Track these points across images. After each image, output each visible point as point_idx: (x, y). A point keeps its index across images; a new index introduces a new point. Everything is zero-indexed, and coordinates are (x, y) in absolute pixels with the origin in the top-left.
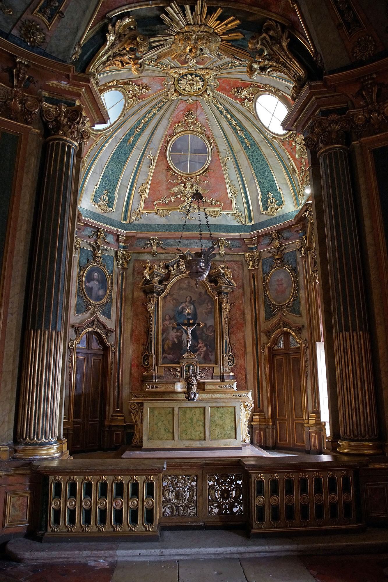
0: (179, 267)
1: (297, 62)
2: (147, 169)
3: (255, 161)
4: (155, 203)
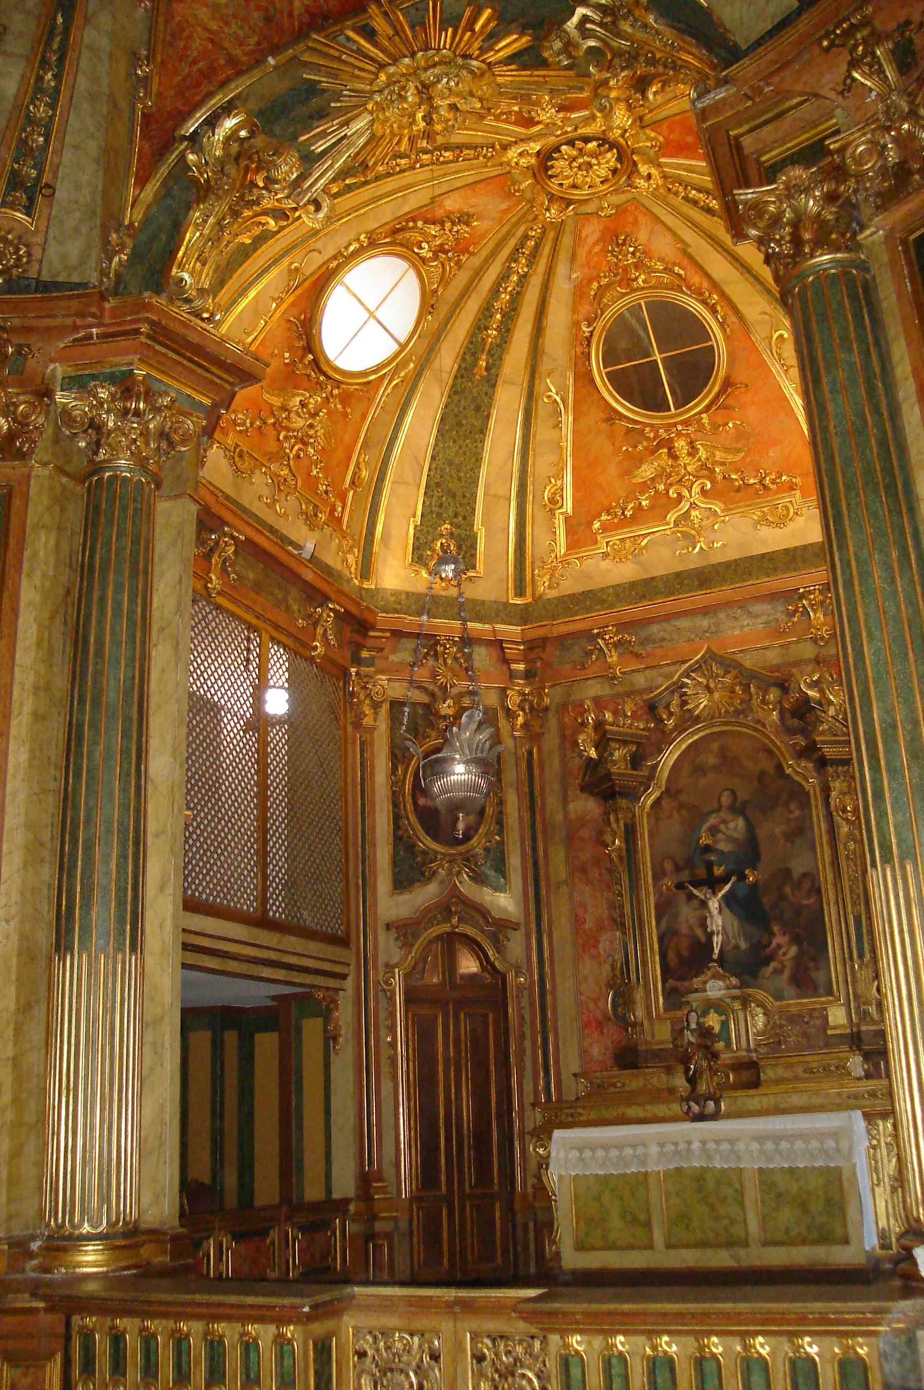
0: (684, 703)
4: (596, 525)
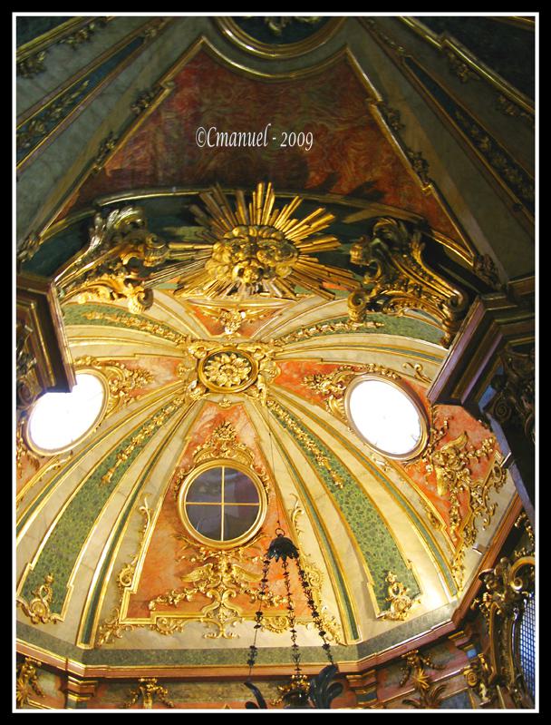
1: (443, 280)
2: (137, 536)
3: (353, 513)
4: (152, 605)
